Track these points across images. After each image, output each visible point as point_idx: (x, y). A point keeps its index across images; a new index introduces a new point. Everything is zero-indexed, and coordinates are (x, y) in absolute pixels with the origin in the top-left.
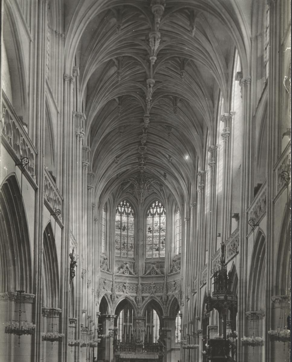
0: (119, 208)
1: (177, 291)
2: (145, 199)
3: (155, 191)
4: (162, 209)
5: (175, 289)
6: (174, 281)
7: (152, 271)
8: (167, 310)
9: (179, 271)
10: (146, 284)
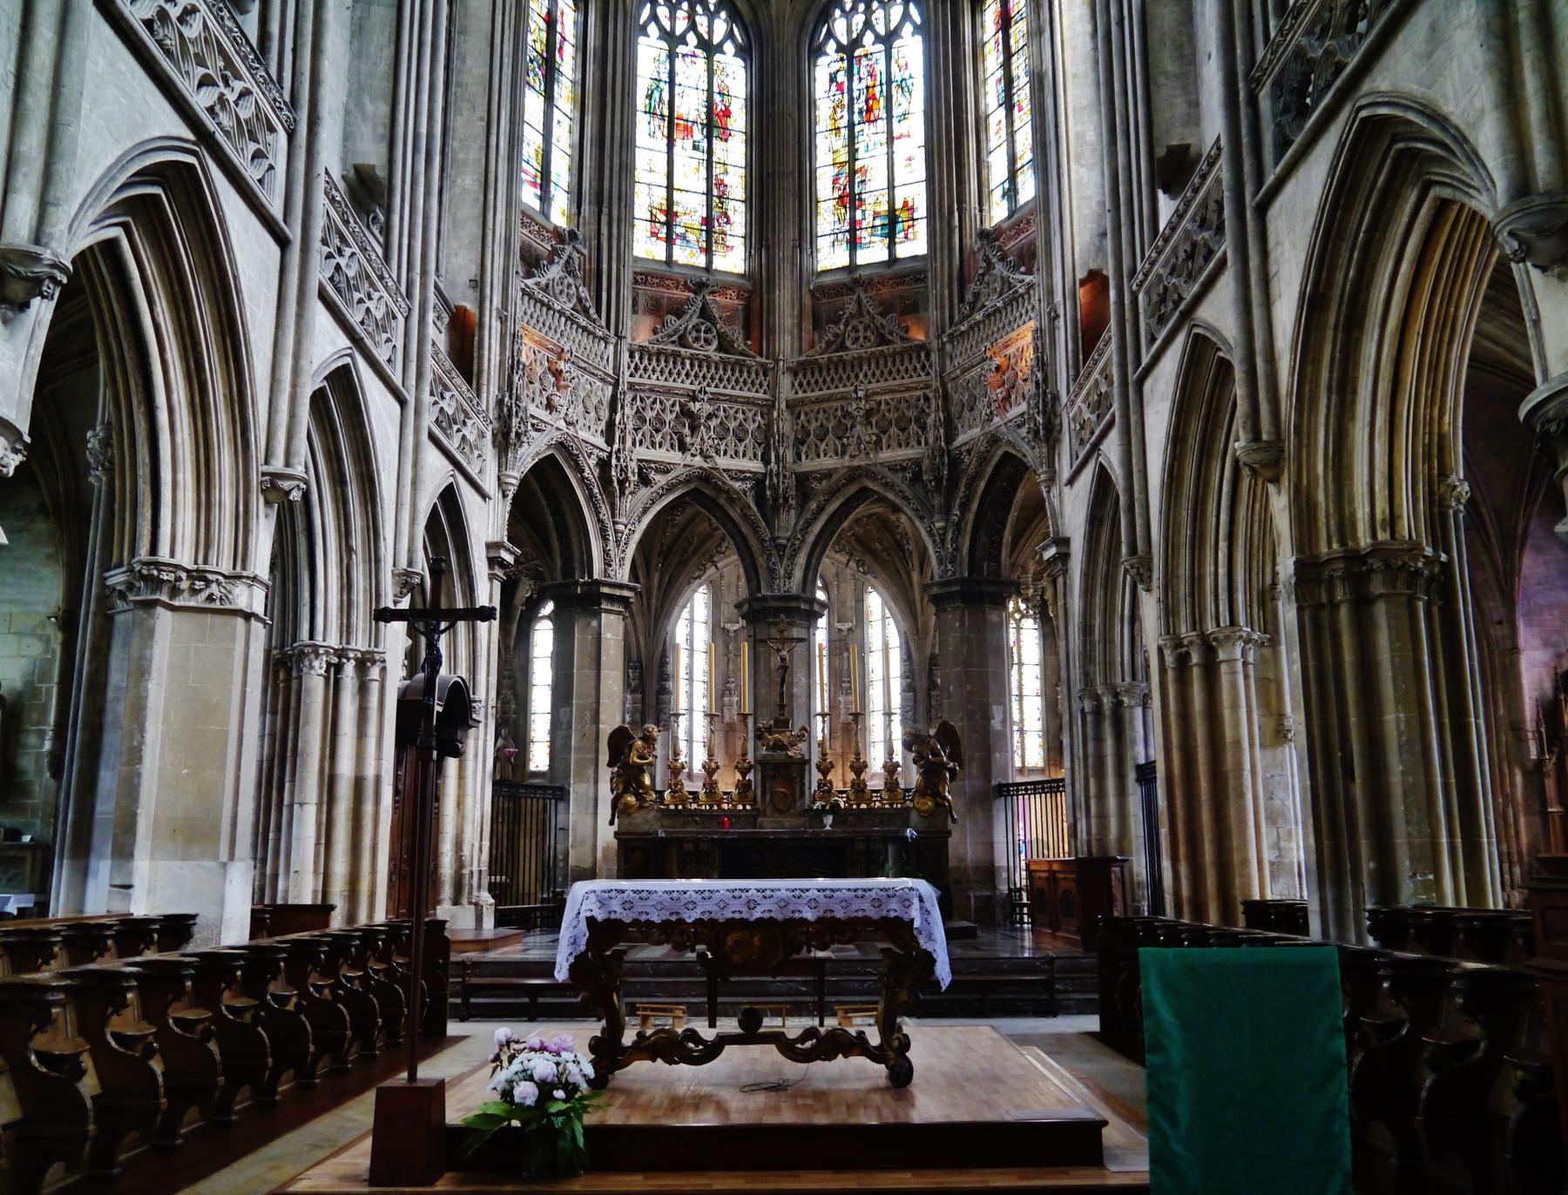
0: (663, 12)
4: (896, 12)
5: (1007, 398)
7: (856, 330)
8: (954, 540)
10: (818, 401)
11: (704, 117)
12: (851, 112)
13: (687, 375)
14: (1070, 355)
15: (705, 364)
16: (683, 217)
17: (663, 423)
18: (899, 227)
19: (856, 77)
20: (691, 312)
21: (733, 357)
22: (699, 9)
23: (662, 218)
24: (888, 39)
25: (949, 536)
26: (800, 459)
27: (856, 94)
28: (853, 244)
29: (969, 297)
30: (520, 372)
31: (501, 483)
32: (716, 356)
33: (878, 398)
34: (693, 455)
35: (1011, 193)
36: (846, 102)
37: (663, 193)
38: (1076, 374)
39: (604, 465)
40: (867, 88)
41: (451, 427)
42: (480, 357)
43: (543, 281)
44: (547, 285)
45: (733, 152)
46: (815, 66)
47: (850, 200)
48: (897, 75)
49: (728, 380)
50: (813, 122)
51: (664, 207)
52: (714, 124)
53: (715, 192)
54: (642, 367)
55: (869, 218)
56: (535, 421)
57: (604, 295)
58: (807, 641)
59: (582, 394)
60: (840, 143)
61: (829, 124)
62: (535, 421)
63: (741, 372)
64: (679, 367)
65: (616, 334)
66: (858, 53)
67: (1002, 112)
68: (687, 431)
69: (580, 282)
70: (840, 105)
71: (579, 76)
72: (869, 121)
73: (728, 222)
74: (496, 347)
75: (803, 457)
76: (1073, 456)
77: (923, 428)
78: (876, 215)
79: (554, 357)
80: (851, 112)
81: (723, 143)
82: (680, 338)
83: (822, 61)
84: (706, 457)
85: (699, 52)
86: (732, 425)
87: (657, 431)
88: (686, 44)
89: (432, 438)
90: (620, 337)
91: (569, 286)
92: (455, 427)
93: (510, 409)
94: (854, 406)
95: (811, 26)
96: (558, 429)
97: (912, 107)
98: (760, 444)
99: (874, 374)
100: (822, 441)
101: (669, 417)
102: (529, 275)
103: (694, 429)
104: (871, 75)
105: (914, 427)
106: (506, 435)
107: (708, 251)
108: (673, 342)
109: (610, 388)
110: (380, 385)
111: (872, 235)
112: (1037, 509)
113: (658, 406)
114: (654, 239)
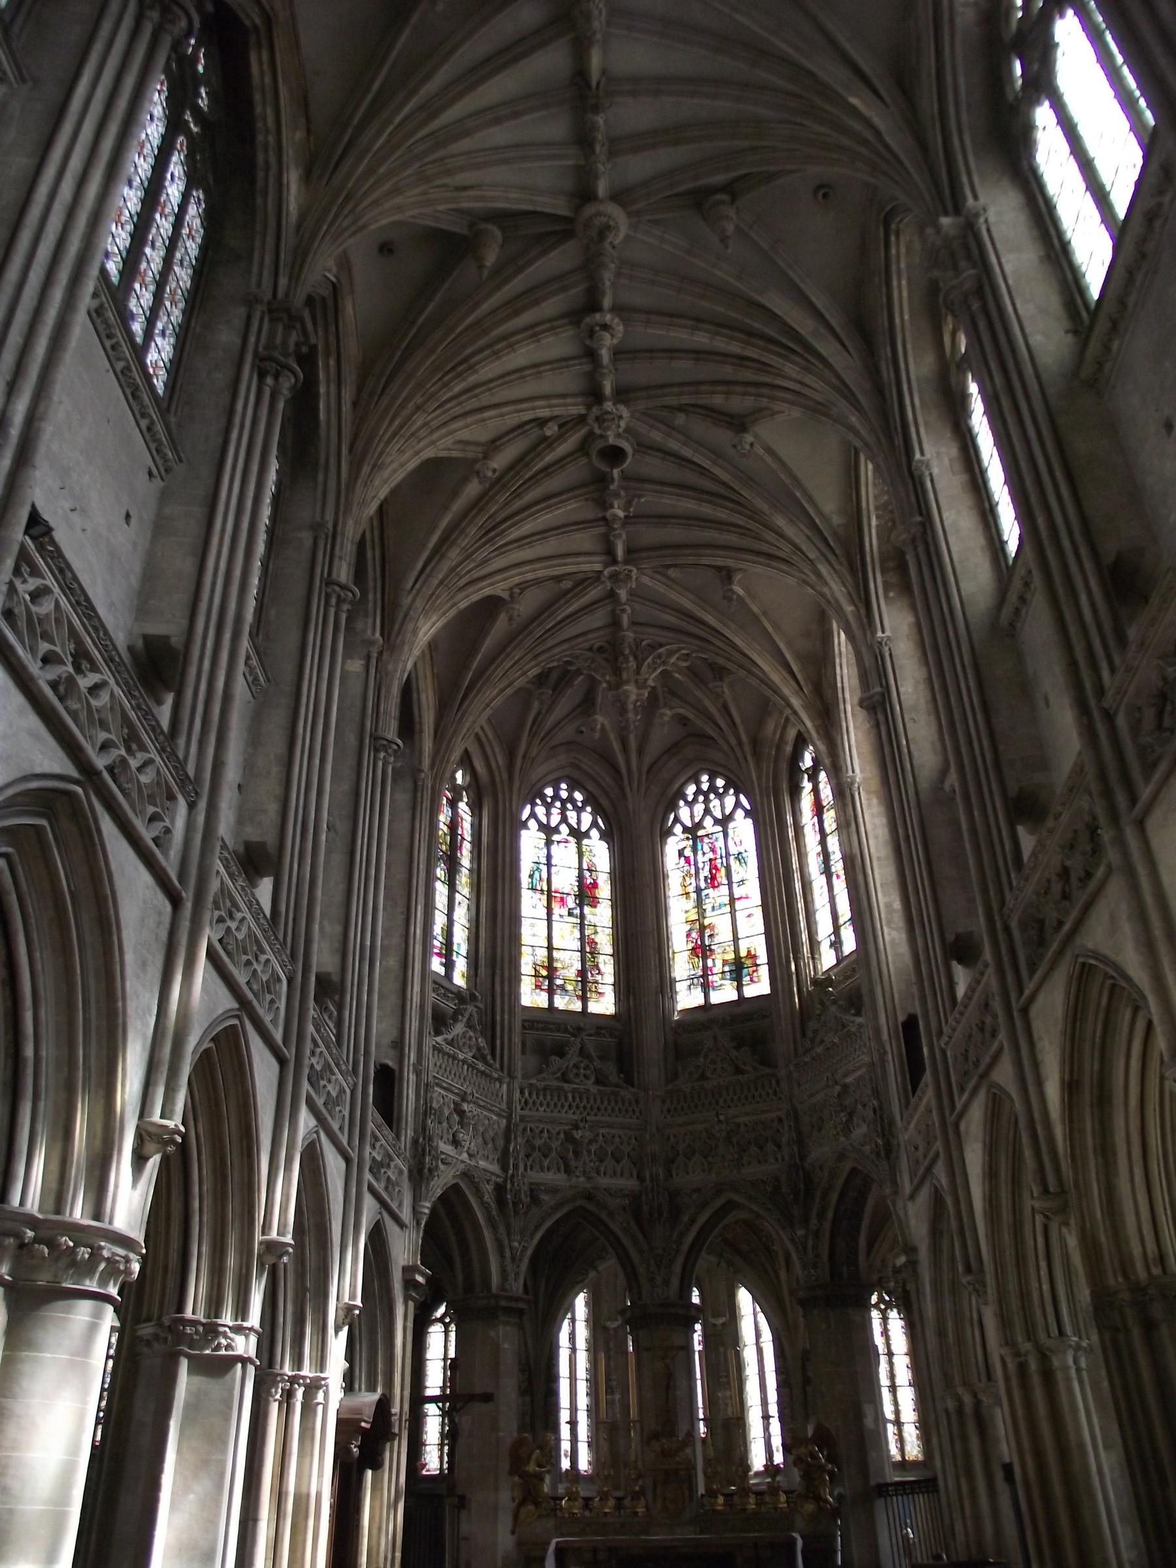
1: (860, 1130)
3: (690, 715)
4: (730, 801)
6: (836, 1083)
9: (859, 1020)
11: (576, 889)
13: (570, 1107)
14: (900, 1086)
15: (584, 1096)
16: (562, 971)
17: (550, 1149)
18: (745, 971)
19: (700, 853)
20: (571, 1052)
21: (608, 1089)
22: (569, 806)
23: (544, 973)
24: (724, 822)
25: (810, 1243)
26: (671, 1176)
27: (700, 865)
28: (706, 987)
29: (810, 1034)
30: (432, 1117)
31: (415, 1212)
32: (594, 1089)
33: (739, 1120)
34: (577, 1177)
35: (837, 944)
36: (693, 872)
37: (545, 952)
38: (906, 1105)
39: (500, 1189)
40: (711, 860)
41: (380, 1171)
42: (400, 1105)
43: (450, 1037)
44: (453, 1039)
45: (602, 916)
46: (666, 843)
47: (701, 951)
48: (733, 850)
49: (606, 1109)
51: (546, 964)
52: (586, 894)
53: (588, 949)
54: (531, 1101)
55: (719, 963)
56: (443, 1156)
57: (498, 1042)
58: (688, 1348)
59: (481, 1129)
60: (691, 903)
62: (443, 1156)
63: (616, 1102)
64: (563, 1100)
65: (509, 1075)
66: (700, 833)
67: (823, 878)
68: (571, 1155)
69: (479, 1034)
70: (688, 874)
71: (475, 866)
72: (714, 887)
73: (599, 973)
74: (412, 1096)
75: (674, 1173)
76: (913, 1174)
77: (779, 1147)
78: (725, 963)
79: (457, 1099)
82: (563, 1074)
83: (671, 841)
84: (589, 1179)
85: (571, 839)
86: (610, 1150)
87: (545, 1156)
88: (559, 832)
89: (371, 1190)
90: (511, 1076)
91: (470, 1038)
92: (383, 1171)
93: (424, 1150)
94: (717, 1128)
96: (463, 1162)
97: (748, 875)
98: (635, 1164)
99: (732, 1100)
100: (689, 1159)
101: (555, 1145)
102: (438, 1032)
103: (577, 1154)
104: (713, 850)
105: (770, 1147)
106: (420, 1172)
107: (584, 999)
108: (557, 1078)
109: (504, 1121)
110: (333, 1149)
111: (723, 979)
112: (884, 1217)
113: (545, 1134)
114: (538, 991)
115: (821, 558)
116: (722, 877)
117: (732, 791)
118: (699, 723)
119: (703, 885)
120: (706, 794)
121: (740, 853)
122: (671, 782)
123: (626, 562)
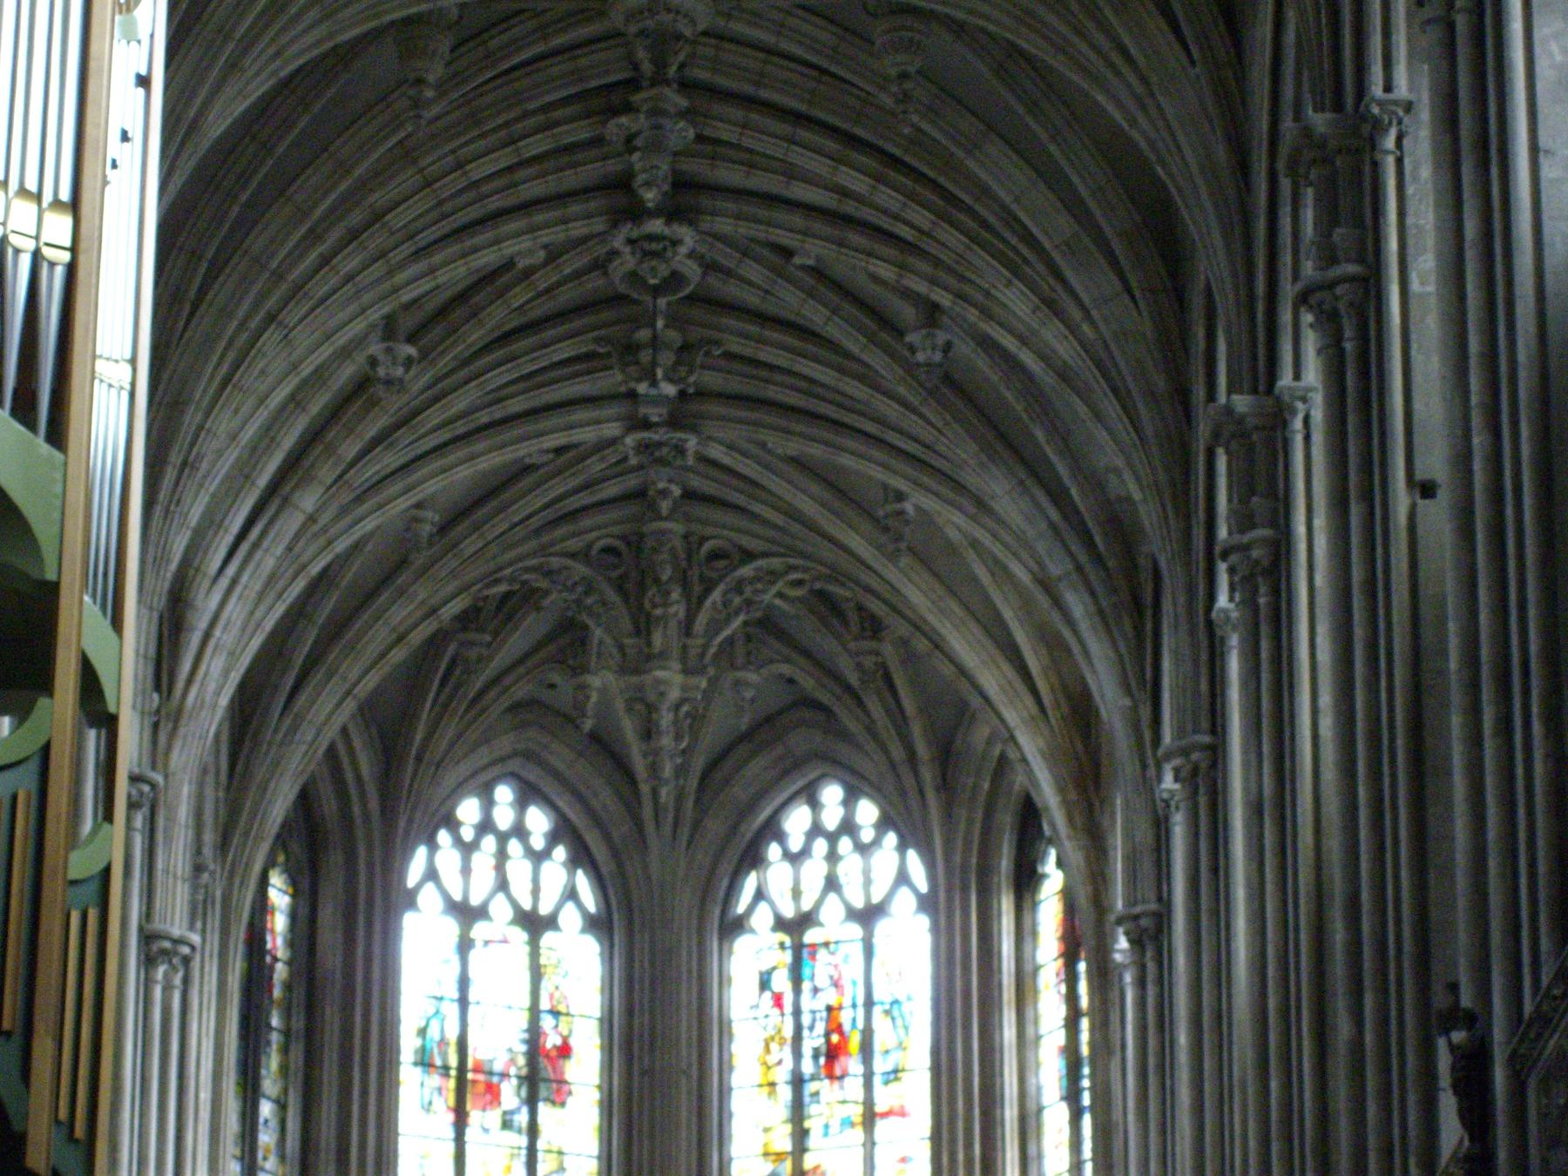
2: (706, 775)
3: (808, 683)
11: (521, 1061)
12: (797, 1054)
19: (806, 986)
22: (514, 847)
24: (868, 916)
27: (806, 1020)
36: (788, 1032)
40: (829, 1009)
46: (730, 953)
50: (725, 1067)
61: (758, 1075)
66: (811, 936)
72: (831, 1076)
80: (797, 1054)
81: (557, 1111)
83: (742, 946)
95: (725, 883)
104: (836, 984)
115: (1074, 576)
116: (854, 1065)
117: (891, 839)
118: (824, 697)
119: (807, 1067)
120: (833, 838)
121: (895, 1002)
122: (752, 806)
123: (674, 422)
